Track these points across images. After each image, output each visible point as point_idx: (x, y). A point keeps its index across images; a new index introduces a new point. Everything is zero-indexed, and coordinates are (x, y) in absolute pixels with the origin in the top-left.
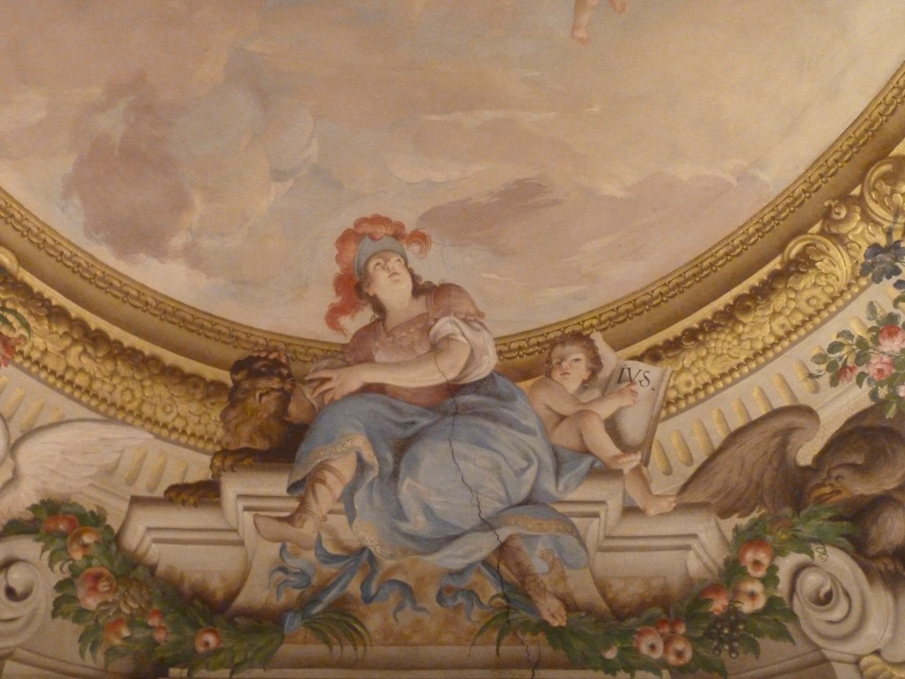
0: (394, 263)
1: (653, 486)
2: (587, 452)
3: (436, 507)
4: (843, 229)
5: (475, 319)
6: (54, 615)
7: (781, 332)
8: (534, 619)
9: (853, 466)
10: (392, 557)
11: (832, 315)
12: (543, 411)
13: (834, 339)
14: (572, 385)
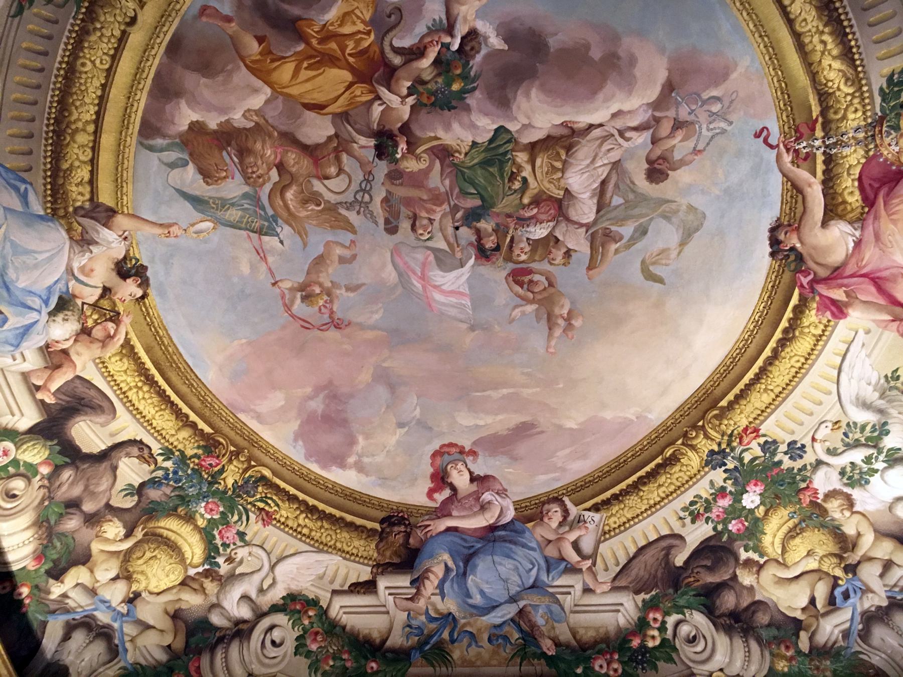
0: (460, 466)
1: (598, 577)
2: (563, 559)
3: (486, 590)
4: (694, 442)
5: (503, 493)
6: (295, 654)
7: (663, 495)
8: (539, 651)
9: (705, 566)
10: (464, 618)
11: (690, 487)
12: (540, 539)
13: (692, 499)
14: (554, 524)
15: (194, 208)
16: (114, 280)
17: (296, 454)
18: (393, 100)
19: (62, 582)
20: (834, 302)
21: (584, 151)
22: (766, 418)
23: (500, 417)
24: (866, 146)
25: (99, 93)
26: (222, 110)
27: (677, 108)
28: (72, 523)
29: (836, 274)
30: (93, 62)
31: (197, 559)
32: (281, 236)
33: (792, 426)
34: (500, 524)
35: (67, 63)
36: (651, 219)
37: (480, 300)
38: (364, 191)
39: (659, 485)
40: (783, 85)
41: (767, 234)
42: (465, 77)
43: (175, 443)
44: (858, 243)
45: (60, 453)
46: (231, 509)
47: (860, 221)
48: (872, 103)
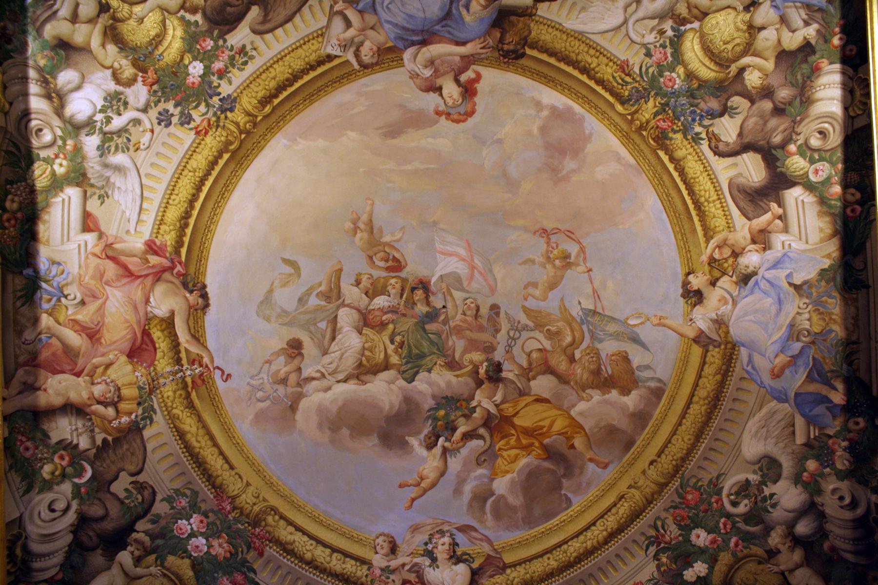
0: (450, 102)
5: (414, 76)
7: (271, 70)
9: (231, 6)
11: (248, 78)
12: (381, 31)
14: (368, 44)
16: (706, 291)
17: (592, 123)
19: (805, 38)
20: (156, 253)
21: (349, 363)
22: (191, 145)
23: (413, 144)
24: (156, 374)
25: (684, 421)
26: (606, 402)
28: (784, 93)
29: (158, 275)
30: (683, 440)
31: (690, 36)
32: (579, 308)
33: (171, 141)
34: (416, 47)
35: (699, 441)
36: (296, 310)
38: (513, 339)
39: (274, 79)
41: (211, 302)
42: (435, 419)
43: (689, 146)
44: (147, 301)
45: (778, 159)
46: (653, 80)
47: (149, 319)
48: (159, 403)
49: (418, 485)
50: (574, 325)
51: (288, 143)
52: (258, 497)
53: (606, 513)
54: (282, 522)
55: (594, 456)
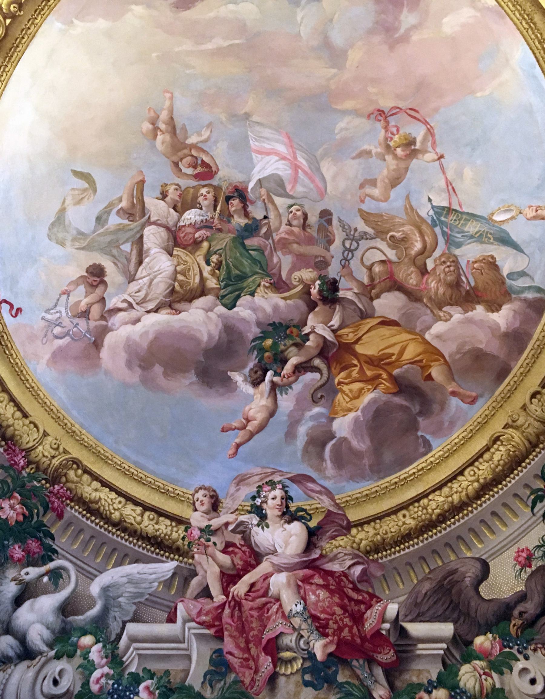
15: (508, 234)
18: (322, 330)
21: (160, 289)
26: (470, 321)
27: (88, 328)
32: (430, 206)
36: (94, 232)
37: (240, 146)
38: (350, 250)
40: (7, 352)
42: (262, 350)
49: (244, 427)
50: (424, 227)
51: (63, 27)
52: (57, 449)
53: (477, 460)
54: (86, 477)
55: (456, 389)
